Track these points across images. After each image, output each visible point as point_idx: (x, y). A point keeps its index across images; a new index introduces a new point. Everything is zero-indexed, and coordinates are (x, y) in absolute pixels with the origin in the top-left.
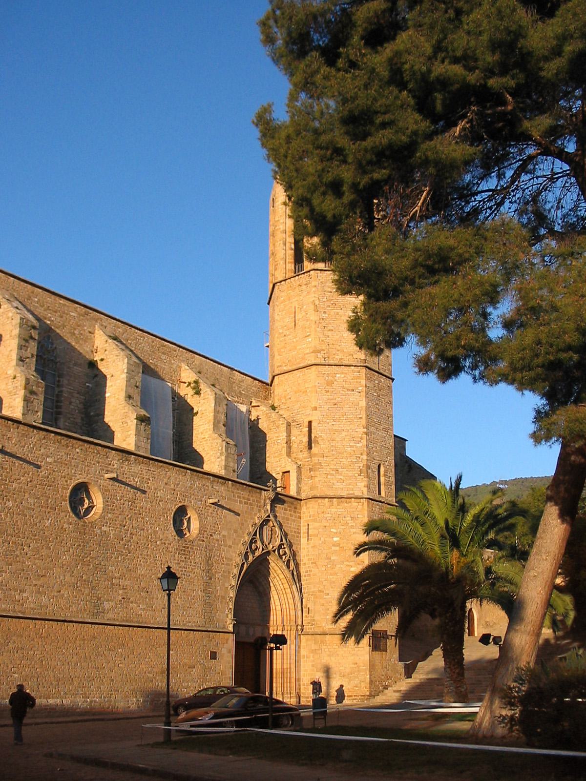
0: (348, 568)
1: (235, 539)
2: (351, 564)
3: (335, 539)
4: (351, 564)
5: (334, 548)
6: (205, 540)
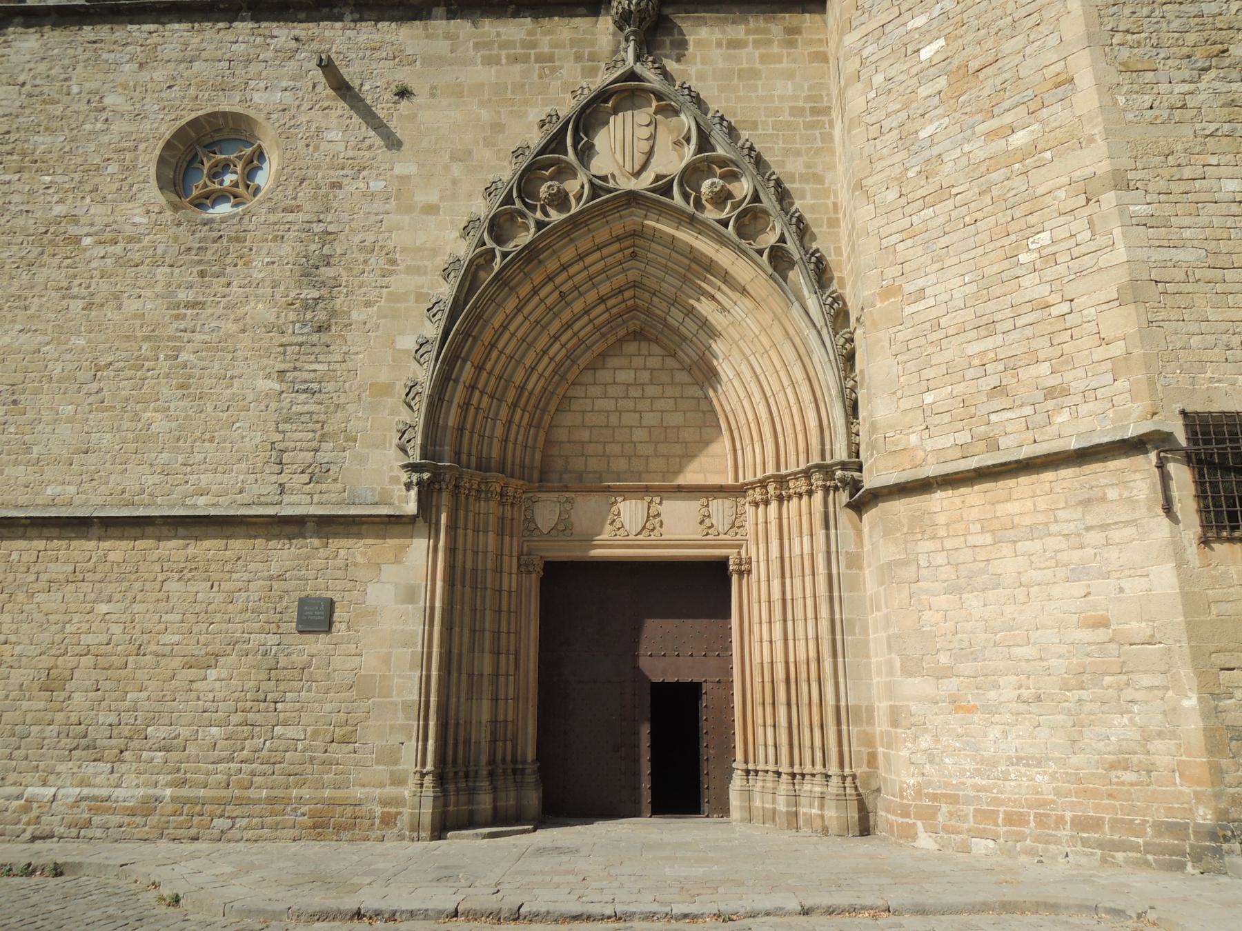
0: (998, 145)
1: (454, 182)
2: (1008, 119)
3: (925, 54)
4: (1008, 119)
5: (923, 91)
6: (307, 206)
